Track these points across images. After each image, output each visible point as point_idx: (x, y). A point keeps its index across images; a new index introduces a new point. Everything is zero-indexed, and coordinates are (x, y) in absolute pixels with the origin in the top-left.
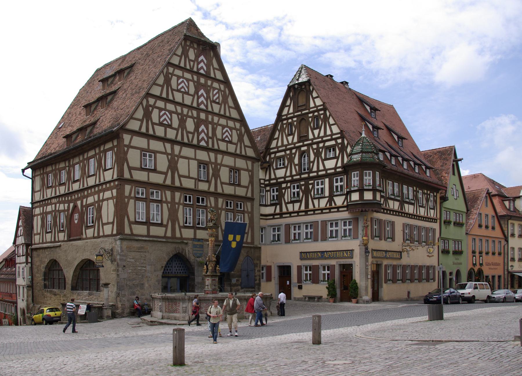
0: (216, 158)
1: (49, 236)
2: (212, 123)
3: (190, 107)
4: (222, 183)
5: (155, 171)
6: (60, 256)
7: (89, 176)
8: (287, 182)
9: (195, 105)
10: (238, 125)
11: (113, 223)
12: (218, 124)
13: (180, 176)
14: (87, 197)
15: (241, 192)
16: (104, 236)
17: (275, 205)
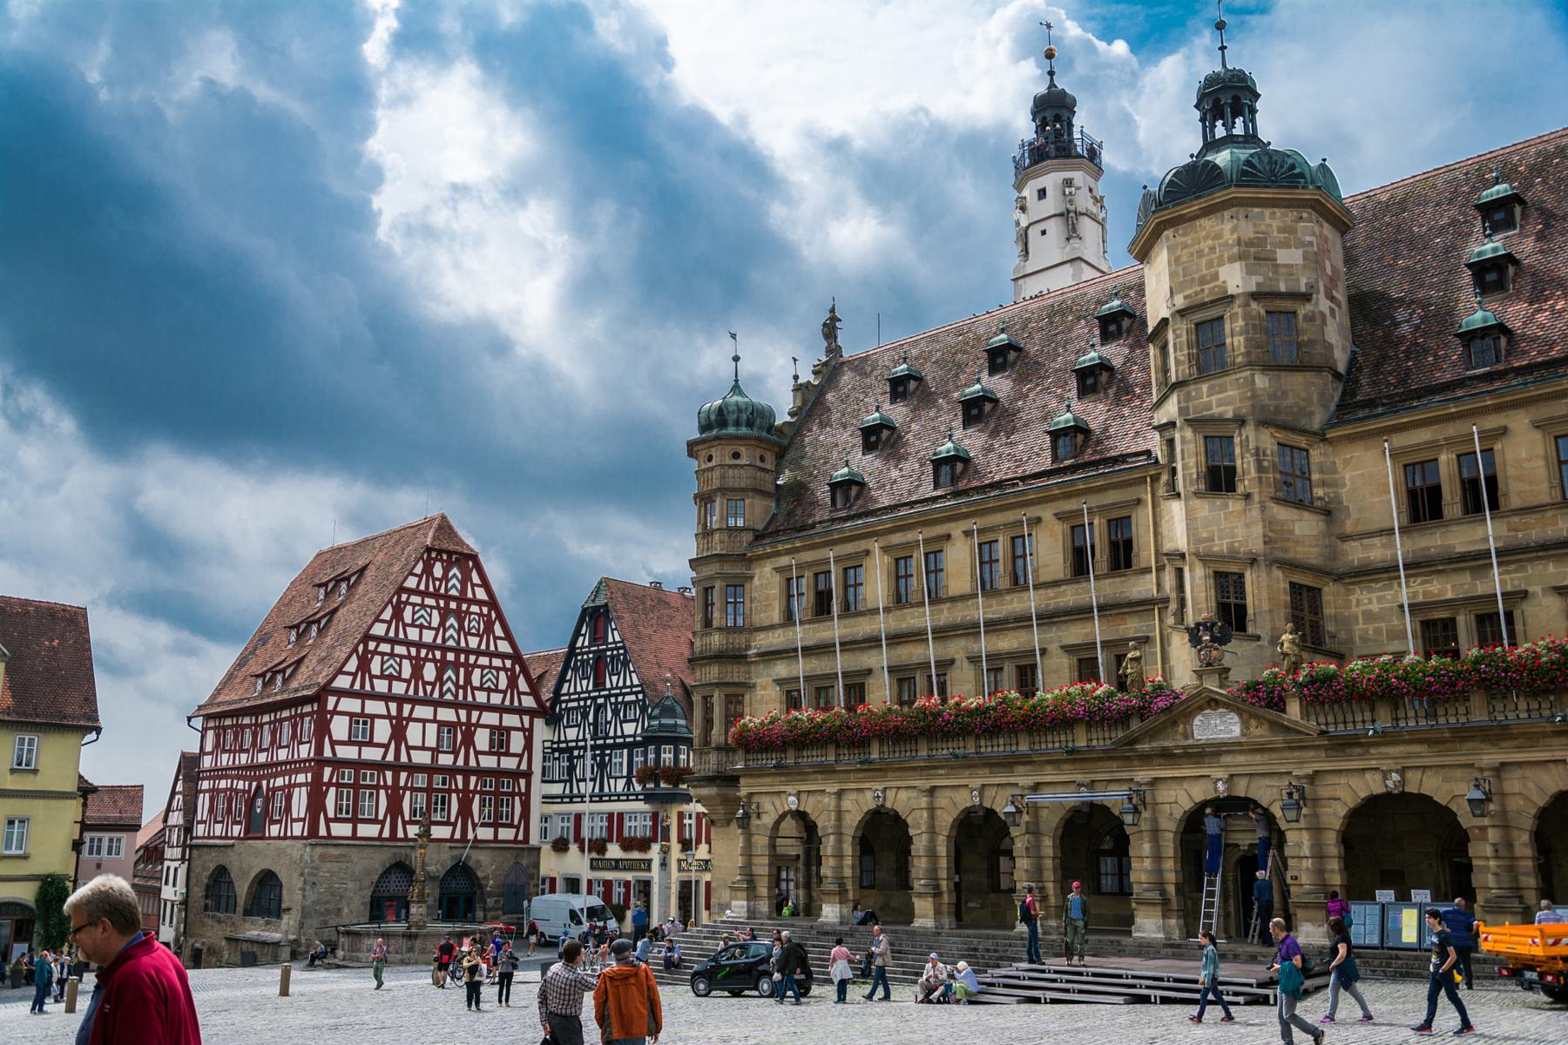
0: (469, 716)
1: (218, 827)
2: (466, 664)
3: (431, 647)
4: (477, 753)
5: (371, 744)
6: (233, 861)
7: (280, 747)
8: (577, 748)
9: (439, 641)
10: (508, 663)
11: (303, 820)
12: (475, 665)
13: (409, 748)
14: (276, 776)
15: (509, 763)
16: (293, 838)
17: (565, 782)
